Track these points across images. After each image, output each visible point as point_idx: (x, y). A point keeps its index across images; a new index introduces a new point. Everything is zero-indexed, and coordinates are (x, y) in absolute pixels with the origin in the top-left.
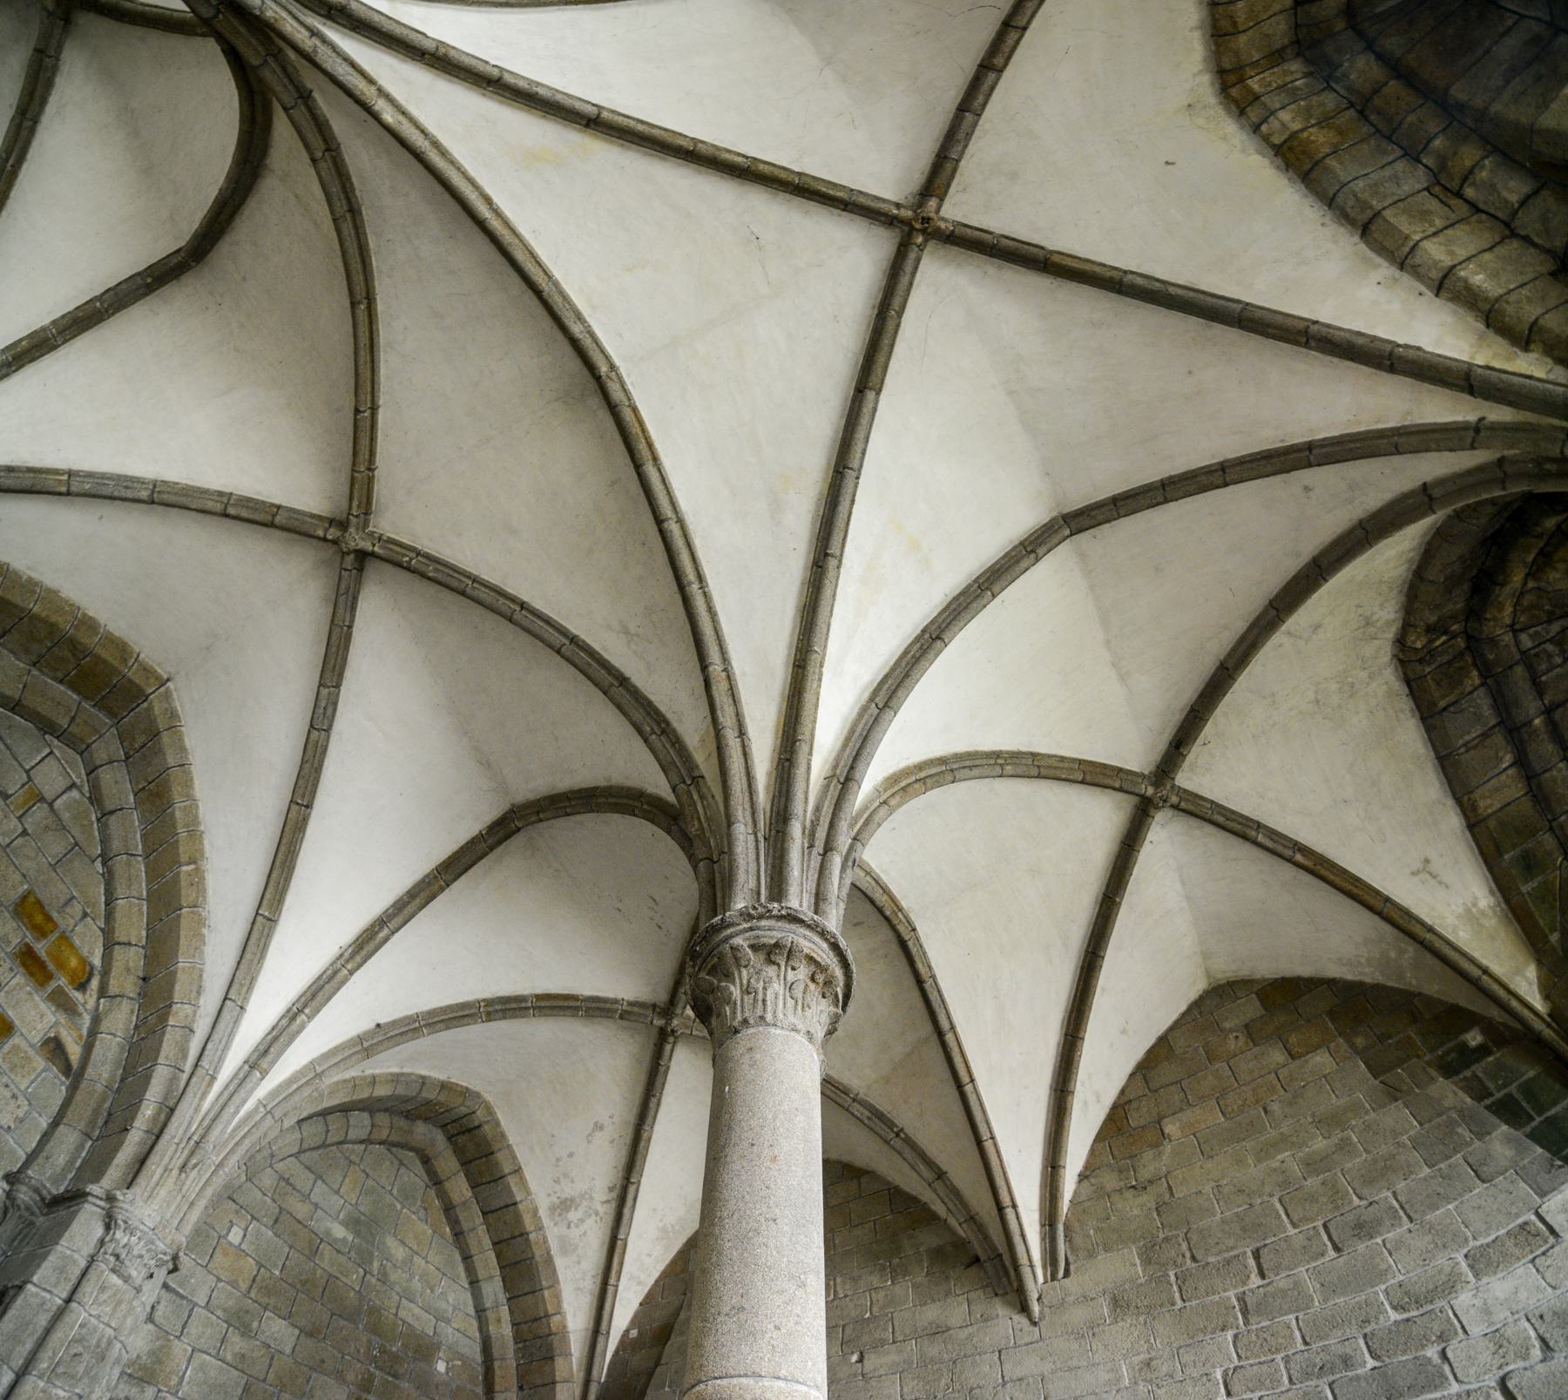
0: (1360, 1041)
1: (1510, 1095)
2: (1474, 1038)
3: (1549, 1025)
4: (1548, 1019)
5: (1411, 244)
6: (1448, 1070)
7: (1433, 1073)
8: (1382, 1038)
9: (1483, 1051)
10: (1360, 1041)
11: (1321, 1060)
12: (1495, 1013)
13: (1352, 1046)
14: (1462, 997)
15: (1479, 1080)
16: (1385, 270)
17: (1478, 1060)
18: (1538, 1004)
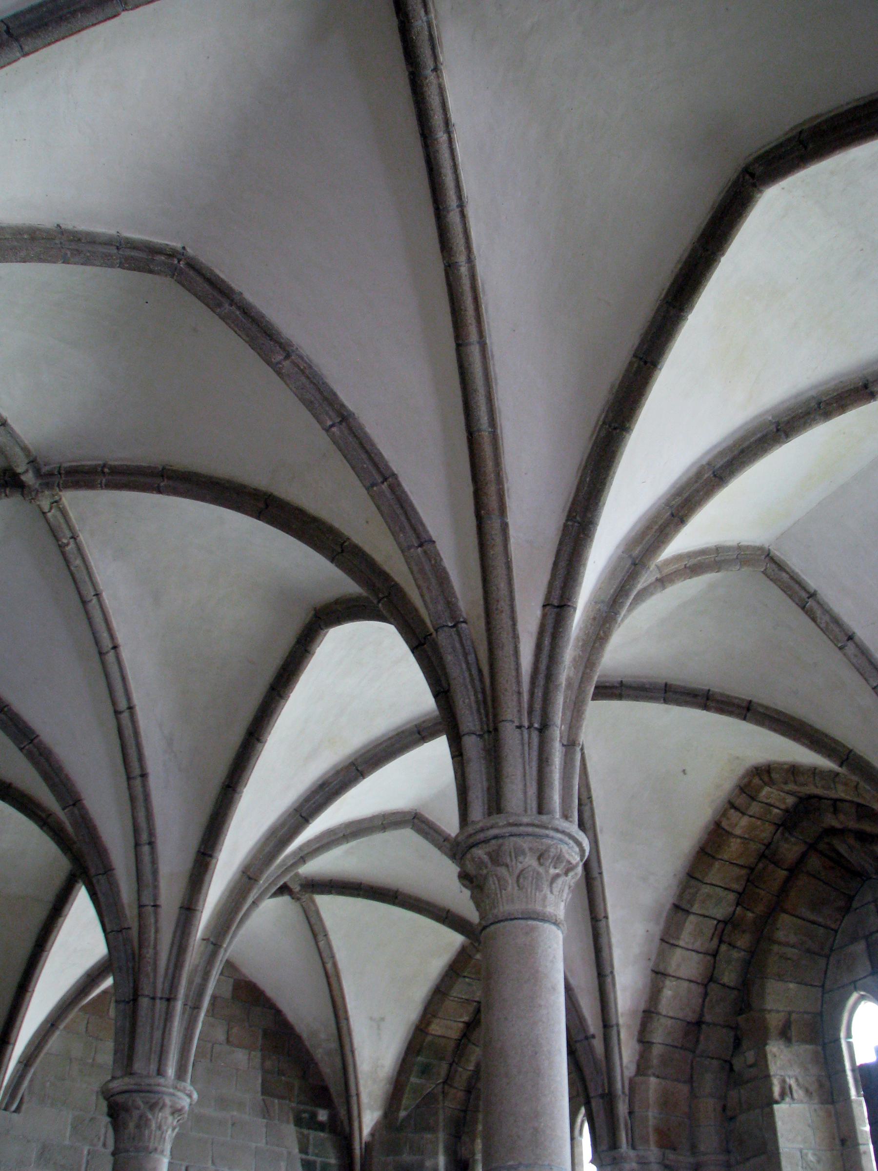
0: (268, 1063)
1: (315, 1162)
2: (323, 1116)
3: (361, 1148)
4: (363, 1146)
5: (676, 943)
6: (299, 1122)
7: (291, 1118)
8: (281, 1072)
9: (321, 1127)
10: (268, 1063)
11: (240, 1056)
12: (342, 1112)
13: (263, 1062)
14: (335, 1090)
15: (308, 1140)
16: (657, 930)
17: (316, 1130)
18: (366, 1130)
